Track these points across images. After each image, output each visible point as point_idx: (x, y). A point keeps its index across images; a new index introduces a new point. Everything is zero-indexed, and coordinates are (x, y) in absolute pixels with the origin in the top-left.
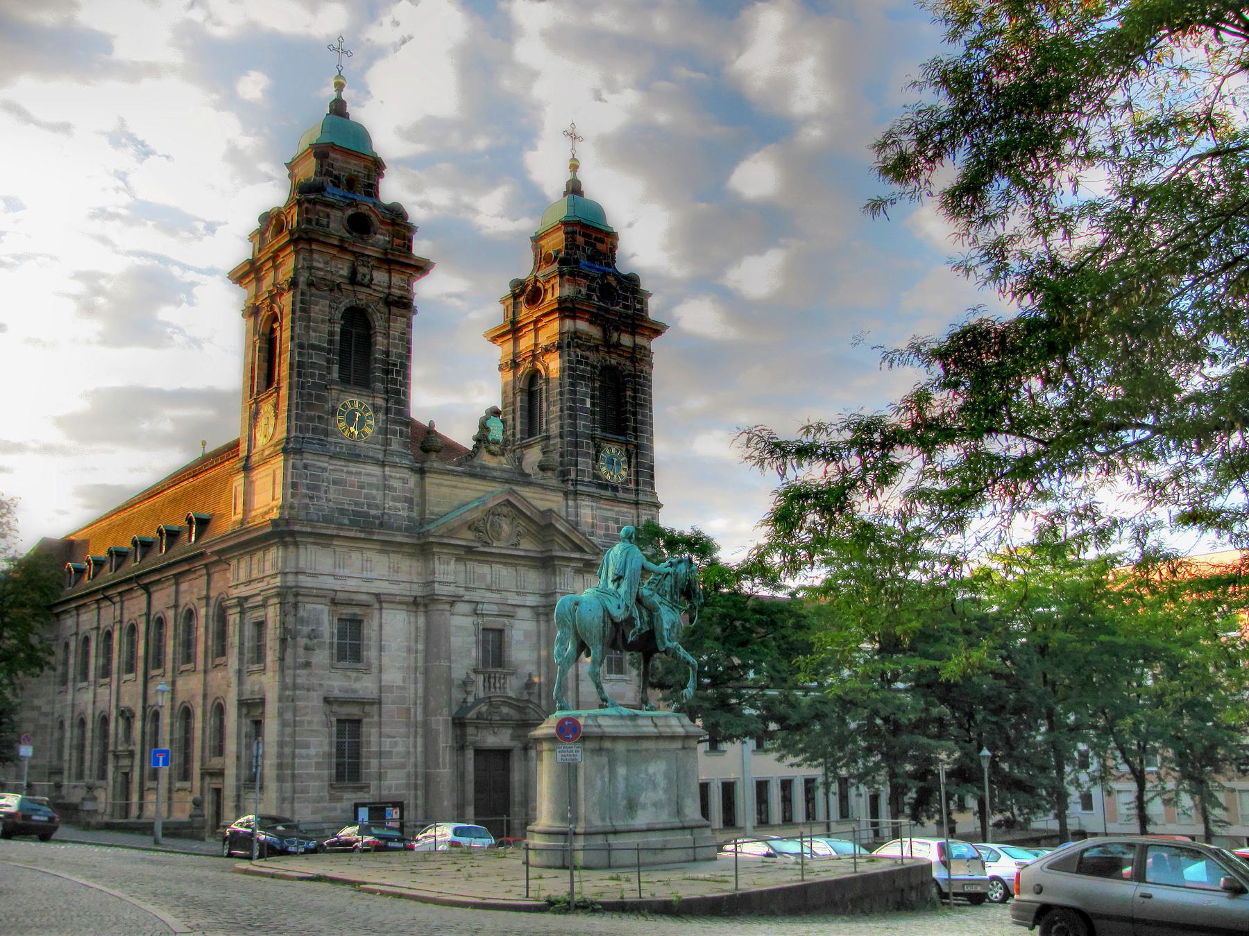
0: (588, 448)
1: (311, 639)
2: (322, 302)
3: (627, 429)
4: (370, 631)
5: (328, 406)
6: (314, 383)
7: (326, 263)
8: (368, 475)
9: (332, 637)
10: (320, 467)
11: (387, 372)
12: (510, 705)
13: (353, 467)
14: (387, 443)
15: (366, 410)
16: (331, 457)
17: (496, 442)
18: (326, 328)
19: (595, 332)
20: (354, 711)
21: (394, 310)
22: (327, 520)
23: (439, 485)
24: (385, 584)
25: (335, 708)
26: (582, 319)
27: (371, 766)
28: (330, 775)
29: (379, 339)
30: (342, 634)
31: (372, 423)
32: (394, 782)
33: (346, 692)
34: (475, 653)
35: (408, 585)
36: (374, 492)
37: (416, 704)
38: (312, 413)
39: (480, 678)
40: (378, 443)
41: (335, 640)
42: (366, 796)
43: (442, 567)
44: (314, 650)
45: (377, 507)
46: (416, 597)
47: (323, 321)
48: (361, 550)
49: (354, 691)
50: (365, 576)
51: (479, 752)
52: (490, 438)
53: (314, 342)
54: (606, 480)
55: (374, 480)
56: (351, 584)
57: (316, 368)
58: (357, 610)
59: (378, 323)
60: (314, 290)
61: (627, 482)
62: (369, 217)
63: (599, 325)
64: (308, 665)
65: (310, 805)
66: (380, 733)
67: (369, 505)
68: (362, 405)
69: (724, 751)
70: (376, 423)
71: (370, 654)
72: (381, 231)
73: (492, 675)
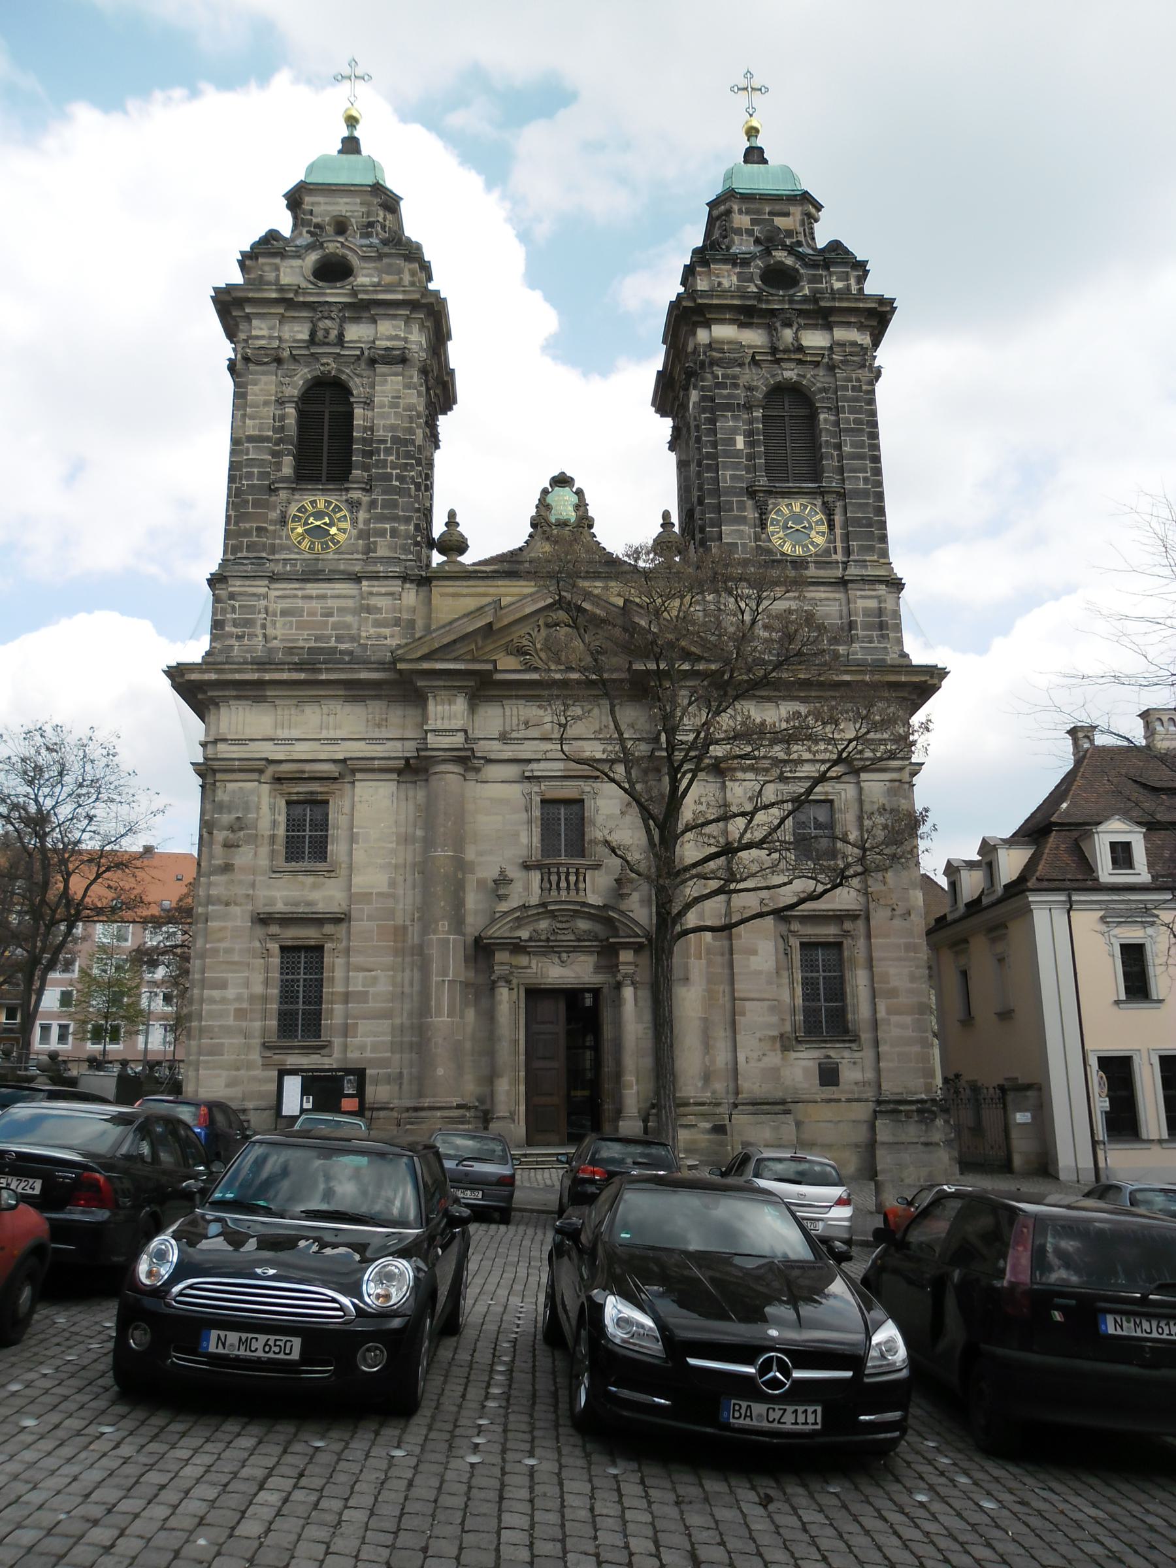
0: (744, 509)
1: (233, 831)
2: (264, 378)
3: (823, 472)
4: (337, 815)
5: (274, 515)
6: (253, 486)
7: (272, 328)
8: (338, 597)
9: (274, 824)
10: (254, 595)
11: (370, 454)
12: (591, 917)
13: (313, 589)
14: (369, 549)
15: (338, 509)
16: (274, 578)
17: (563, 524)
18: (270, 411)
19: (753, 338)
20: (309, 934)
21: (381, 369)
22: (262, 664)
23: (454, 595)
24: (361, 745)
25: (274, 929)
26: (721, 321)
27: (335, 1014)
28: (264, 1030)
29: (358, 411)
30: (293, 824)
31: (346, 525)
32: (369, 1040)
33: (297, 904)
34: (528, 840)
35: (399, 744)
36: (349, 619)
37: (413, 920)
38: (247, 525)
39: (536, 876)
40: (358, 553)
41: (281, 831)
42: (326, 1060)
43: (440, 708)
44: (238, 846)
45: (353, 639)
46: (407, 759)
47: (266, 403)
48: (316, 700)
49: (309, 904)
50: (324, 734)
51: (535, 994)
52: (553, 519)
53: (251, 432)
54: (783, 554)
55: (350, 603)
56: (302, 751)
57: (247, 466)
58: (315, 787)
59: (358, 388)
60: (252, 367)
61: (827, 552)
62: (344, 257)
63: (758, 326)
64: (227, 868)
65: (224, 1073)
66: (348, 963)
67: (339, 639)
68: (330, 503)
69: (1160, 1001)
70: (354, 522)
71: (337, 848)
72: (365, 272)
73: (554, 870)
